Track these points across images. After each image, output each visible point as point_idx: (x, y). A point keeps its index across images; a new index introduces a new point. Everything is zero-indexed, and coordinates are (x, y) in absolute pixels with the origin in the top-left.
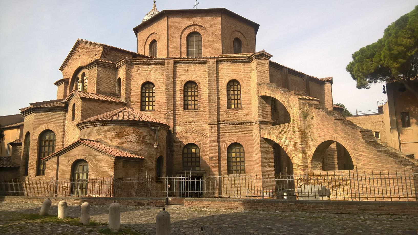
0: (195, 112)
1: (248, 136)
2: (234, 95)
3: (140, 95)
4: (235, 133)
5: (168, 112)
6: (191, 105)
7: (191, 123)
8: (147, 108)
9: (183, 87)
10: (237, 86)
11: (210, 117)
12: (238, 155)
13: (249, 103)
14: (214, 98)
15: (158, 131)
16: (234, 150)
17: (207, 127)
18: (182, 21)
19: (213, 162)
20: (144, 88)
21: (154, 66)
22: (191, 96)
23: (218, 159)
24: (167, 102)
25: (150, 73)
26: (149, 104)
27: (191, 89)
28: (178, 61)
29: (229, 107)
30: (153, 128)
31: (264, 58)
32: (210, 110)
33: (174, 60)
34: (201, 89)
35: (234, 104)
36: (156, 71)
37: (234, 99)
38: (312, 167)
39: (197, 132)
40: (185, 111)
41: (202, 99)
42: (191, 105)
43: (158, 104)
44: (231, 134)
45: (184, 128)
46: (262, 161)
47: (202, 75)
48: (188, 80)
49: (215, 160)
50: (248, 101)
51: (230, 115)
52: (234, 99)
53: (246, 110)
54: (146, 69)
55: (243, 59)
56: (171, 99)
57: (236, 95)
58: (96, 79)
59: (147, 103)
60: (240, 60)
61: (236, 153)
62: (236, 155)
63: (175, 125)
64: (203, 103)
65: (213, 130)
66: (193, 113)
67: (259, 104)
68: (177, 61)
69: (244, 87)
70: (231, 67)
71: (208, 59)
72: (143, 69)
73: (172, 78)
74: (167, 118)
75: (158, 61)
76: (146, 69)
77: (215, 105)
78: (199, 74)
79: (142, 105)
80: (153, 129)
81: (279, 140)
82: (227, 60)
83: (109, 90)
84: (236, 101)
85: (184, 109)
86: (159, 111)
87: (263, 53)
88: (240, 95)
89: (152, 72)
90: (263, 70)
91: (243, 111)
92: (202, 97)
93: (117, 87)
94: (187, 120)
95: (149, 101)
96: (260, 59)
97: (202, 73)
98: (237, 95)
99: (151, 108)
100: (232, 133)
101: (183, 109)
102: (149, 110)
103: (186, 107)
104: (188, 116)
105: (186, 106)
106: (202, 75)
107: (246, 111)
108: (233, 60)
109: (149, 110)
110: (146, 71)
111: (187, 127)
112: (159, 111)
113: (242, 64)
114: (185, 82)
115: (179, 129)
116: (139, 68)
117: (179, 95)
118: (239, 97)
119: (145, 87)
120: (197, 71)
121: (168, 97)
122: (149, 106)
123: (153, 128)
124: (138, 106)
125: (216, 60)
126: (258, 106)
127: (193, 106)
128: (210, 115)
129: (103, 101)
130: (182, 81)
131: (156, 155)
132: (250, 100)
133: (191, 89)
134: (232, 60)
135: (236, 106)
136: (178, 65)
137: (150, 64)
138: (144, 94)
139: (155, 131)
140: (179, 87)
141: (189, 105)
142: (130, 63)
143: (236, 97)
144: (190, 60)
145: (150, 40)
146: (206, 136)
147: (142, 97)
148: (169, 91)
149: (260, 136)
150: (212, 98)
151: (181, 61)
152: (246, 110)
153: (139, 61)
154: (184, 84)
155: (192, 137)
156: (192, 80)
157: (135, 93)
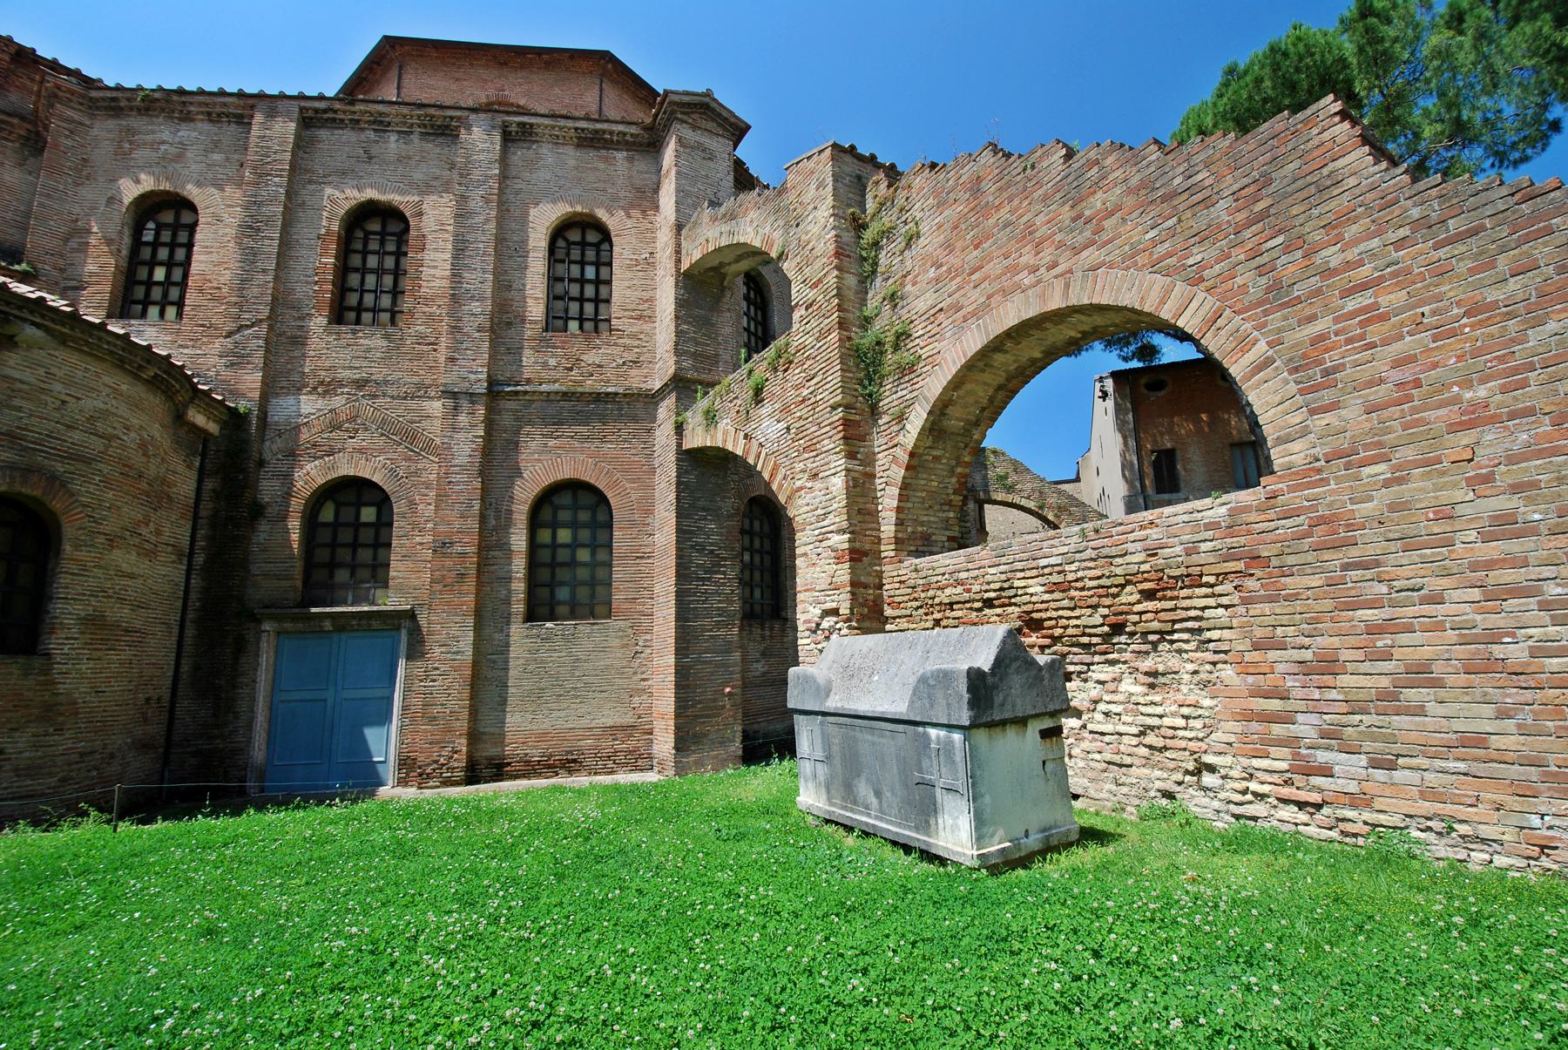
0: (387, 337)
1: (633, 451)
2: (582, 281)
4: (572, 437)
5: (240, 328)
7: (360, 384)
10: (597, 246)
11: (452, 360)
12: (585, 535)
13: (645, 313)
14: (480, 279)
16: (564, 515)
18: (454, 87)
19: (448, 563)
21: (206, 126)
22: (380, 272)
23: (474, 549)
25: (179, 157)
27: (382, 243)
28: (325, 111)
29: (555, 321)
31: (711, 125)
33: (303, 104)
36: (216, 145)
37: (581, 300)
38: (900, 535)
39: (388, 429)
40: (336, 327)
41: (424, 284)
43: (201, 291)
44: (552, 443)
45: (320, 403)
46: (678, 557)
47: (434, 183)
49: (463, 555)
50: (640, 307)
52: (581, 300)
53: (627, 341)
54: (166, 136)
55: (625, 134)
56: (264, 271)
57: (589, 281)
59: (157, 293)
60: (611, 133)
61: (574, 525)
62: (575, 537)
64: (428, 301)
65: (463, 419)
66: (373, 340)
68: (316, 111)
69: (622, 251)
70: (572, 163)
71: (466, 113)
72: (149, 138)
73: (281, 176)
74: (235, 355)
75: (225, 104)
77: (478, 310)
78: (420, 176)
81: (746, 436)
82: (553, 127)
84: (589, 308)
86: (202, 326)
87: (707, 100)
88: (609, 282)
90: (707, 176)
91: (616, 344)
96: (694, 128)
97: (438, 172)
98: (598, 282)
100: (558, 437)
103: (340, 314)
104: (346, 354)
106: (434, 183)
107: (627, 348)
108: (583, 130)
110: (163, 147)
111: (338, 401)
112: (202, 326)
113: (620, 155)
116: (130, 131)
118: (603, 290)
119: (155, 221)
120: (413, 163)
121: (250, 257)
124: (99, 297)
125: (504, 122)
132: (651, 300)
133: (382, 243)
134: (576, 129)
136: (323, 134)
141: (367, 310)
142: (81, 104)
143: (589, 291)
144: (381, 114)
146: (429, 447)
149: (679, 445)
151: (335, 112)
152: (627, 341)
153: (128, 100)
155: (361, 451)
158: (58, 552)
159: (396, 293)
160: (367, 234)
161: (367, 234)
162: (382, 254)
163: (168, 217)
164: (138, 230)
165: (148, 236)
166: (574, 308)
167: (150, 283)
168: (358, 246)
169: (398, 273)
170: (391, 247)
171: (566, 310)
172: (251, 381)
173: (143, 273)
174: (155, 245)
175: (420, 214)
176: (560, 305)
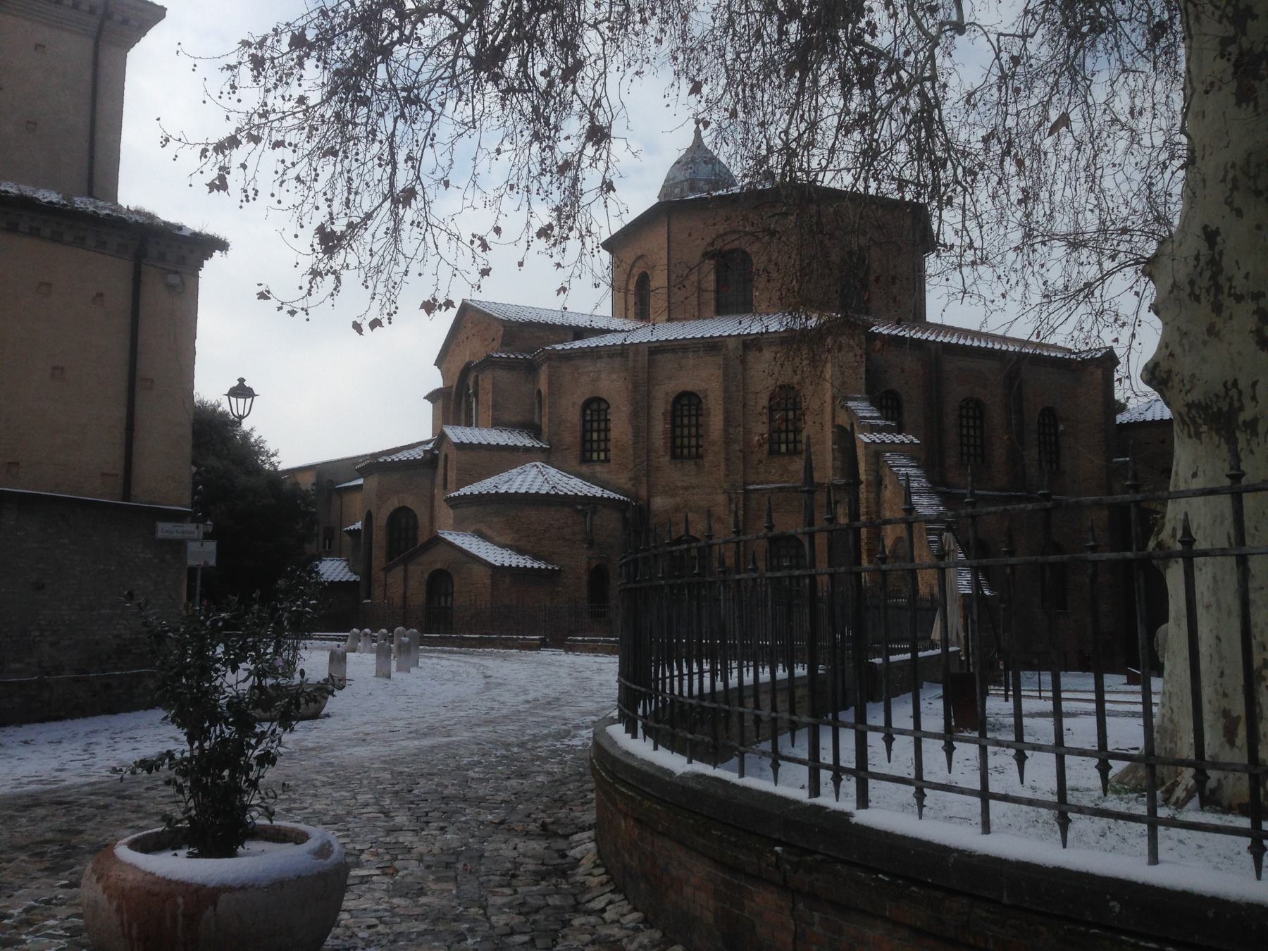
0: (696, 464)
3: (579, 428)
6: (689, 447)
7: (686, 488)
8: (595, 456)
9: (669, 408)
11: (727, 476)
15: (594, 513)
17: (721, 498)
20: (589, 412)
26: (599, 446)
27: (689, 410)
30: (579, 507)
32: (727, 460)
35: (787, 443)
37: (787, 431)
42: (689, 447)
43: (616, 447)
48: (681, 388)
51: (773, 471)
54: (591, 368)
58: (490, 395)
59: (595, 446)
63: (650, 495)
67: (834, 443)
76: (591, 368)
79: (584, 451)
80: (581, 510)
85: (674, 456)
89: (603, 376)
93: (537, 411)
95: (599, 440)
99: (602, 456)
101: (668, 458)
103: (677, 453)
111: (678, 499)
115: (659, 502)
117: (660, 427)
122: (599, 451)
123: (579, 507)
126: (833, 450)
127: (694, 450)
129: (498, 447)
130: (667, 394)
133: (689, 410)
136: (659, 357)
137: (600, 357)
140: (660, 408)
145: (636, 272)
147: (584, 432)
150: (731, 430)
154: (671, 400)
156: (689, 388)
157: (569, 425)
159: (698, 436)
160: (682, 406)
162: (690, 416)
163: (595, 406)
164: (584, 414)
165: (588, 418)
166: (783, 436)
167: (592, 441)
168: (678, 413)
169: (698, 426)
170: (693, 412)
171: (779, 438)
173: (588, 437)
174: (592, 421)
175: (706, 396)
176: (776, 436)
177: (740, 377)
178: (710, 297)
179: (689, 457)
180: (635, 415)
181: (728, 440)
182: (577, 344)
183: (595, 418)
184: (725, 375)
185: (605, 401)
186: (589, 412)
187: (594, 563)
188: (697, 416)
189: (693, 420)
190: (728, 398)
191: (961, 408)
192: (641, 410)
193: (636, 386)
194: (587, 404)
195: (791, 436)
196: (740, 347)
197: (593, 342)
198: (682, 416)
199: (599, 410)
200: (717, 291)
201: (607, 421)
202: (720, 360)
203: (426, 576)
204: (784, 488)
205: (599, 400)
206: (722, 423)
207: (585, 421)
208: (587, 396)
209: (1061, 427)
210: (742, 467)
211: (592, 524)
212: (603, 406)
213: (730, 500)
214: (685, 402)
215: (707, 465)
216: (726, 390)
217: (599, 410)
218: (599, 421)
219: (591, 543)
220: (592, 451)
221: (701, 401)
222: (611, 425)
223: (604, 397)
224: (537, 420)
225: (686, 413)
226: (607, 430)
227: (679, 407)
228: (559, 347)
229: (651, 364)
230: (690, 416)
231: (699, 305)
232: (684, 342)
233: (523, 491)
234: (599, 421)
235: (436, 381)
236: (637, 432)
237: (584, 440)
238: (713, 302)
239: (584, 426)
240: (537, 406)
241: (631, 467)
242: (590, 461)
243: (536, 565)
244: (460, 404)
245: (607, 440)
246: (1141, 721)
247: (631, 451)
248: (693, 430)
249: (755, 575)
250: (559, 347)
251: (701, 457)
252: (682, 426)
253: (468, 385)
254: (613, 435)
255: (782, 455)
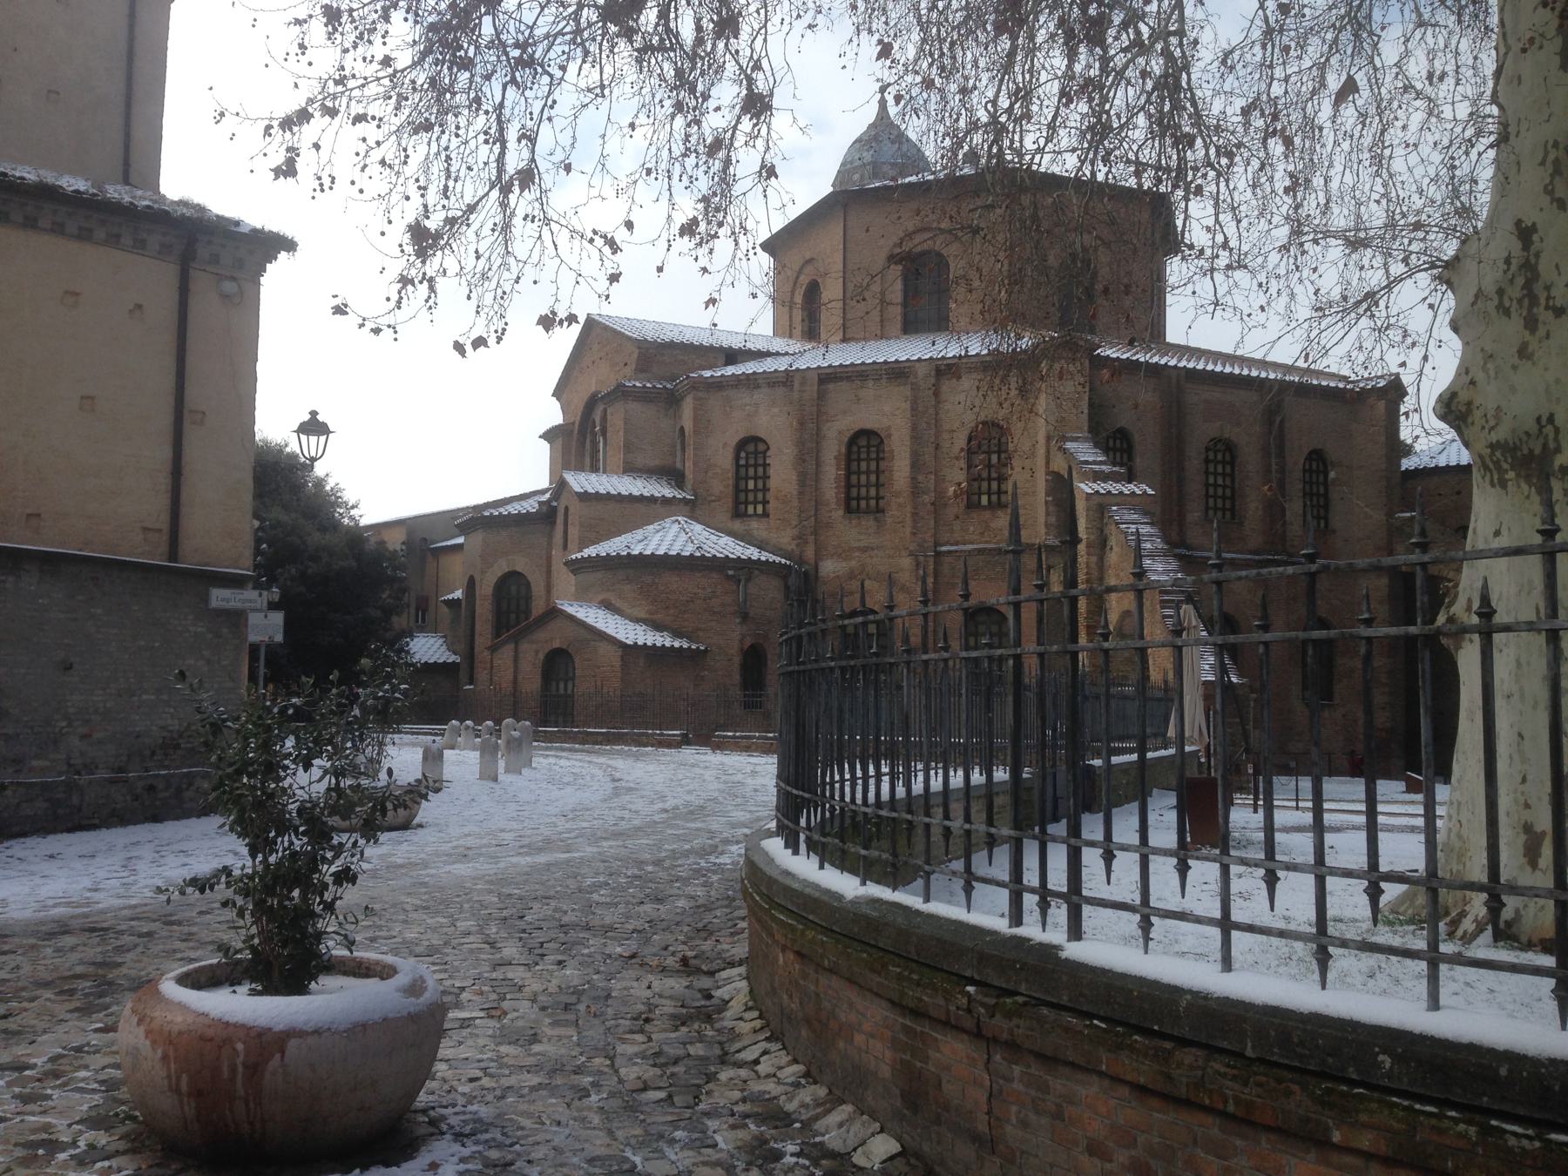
0: (876, 519)
6: (867, 498)
7: (864, 550)
8: (751, 509)
9: (843, 450)
15: (748, 580)
16: (982, 628)
17: (906, 562)
20: (743, 454)
24: (800, 493)
26: (755, 497)
27: (868, 453)
32: (915, 514)
34: (892, 451)
37: (990, 479)
42: (867, 498)
43: (777, 498)
45: (844, 564)
48: (857, 427)
58: (621, 433)
66: (869, 522)
67: (1047, 495)
79: (737, 502)
83: (657, 462)
85: (849, 510)
92: (896, 475)
93: (679, 453)
94: (857, 545)
95: (756, 490)
99: (760, 509)
101: (841, 512)
102: (755, 514)
103: (851, 505)
105: (854, 503)
109: (755, 514)
111: (853, 563)
114: (848, 435)
115: (829, 567)
117: (831, 473)
122: (755, 503)
126: (1046, 502)
127: (873, 502)
128: (914, 527)
129: (631, 499)
131: (742, 641)
133: (868, 453)
135: (994, 498)
136: (831, 386)
137: (758, 387)
138: (743, 471)
139: (739, 581)
140: (832, 450)
145: (804, 280)
147: (738, 478)
148: (804, 461)
150: (920, 478)
156: (868, 426)
157: (719, 471)
158: (766, 665)
159: (878, 485)
161: (859, 448)
162: (868, 460)
163: (751, 448)
164: (737, 458)
165: (742, 462)
166: (985, 485)
167: (747, 491)
168: (854, 456)
169: (878, 472)
170: (873, 456)
172: (810, 553)
174: (747, 466)
175: (890, 436)
176: (976, 484)
177: (932, 411)
178: (896, 312)
179: (868, 511)
180: (801, 459)
181: (916, 490)
182: (730, 370)
183: (752, 461)
184: (914, 409)
185: (764, 442)
186: (743, 454)
187: (748, 642)
188: (878, 460)
189: (873, 465)
190: (916, 436)
191: (1207, 449)
192: (808, 454)
193: (802, 424)
194: (742, 444)
195: (994, 485)
196: (933, 373)
197: (750, 367)
198: (859, 460)
199: (756, 453)
200: (905, 304)
201: (765, 465)
202: (906, 391)
203: (541, 656)
204: (985, 549)
205: (756, 440)
206: (908, 469)
207: (738, 466)
208: (742, 435)
209: (1332, 475)
210: (932, 522)
211: (746, 593)
212: (761, 447)
213: (918, 565)
214: (863, 442)
215: (889, 520)
216: (914, 428)
217: (756, 453)
218: (756, 466)
219: (745, 617)
220: (746, 503)
221: (882, 441)
222: (771, 472)
223: (762, 435)
224: (679, 465)
225: (863, 456)
226: (766, 477)
227: (855, 449)
228: (707, 374)
229: (821, 396)
230: (868, 460)
231: (882, 321)
232: (863, 368)
233: (661, 552)
234: (756, 466)
235: (554, 415)
236: (802, 483)
237: (737, 490)
238: (899, 318)
239: (737, 472)
240: (679, 447)
241: (794, 523)
242: (745, 515)
243: (677, 644)
244: (583, 444)
245: (765, 490)
246: (1422, 837)
247: (796, 503)
248: (873, 478)
249: (946, 655)
250: (707, 374)
251: (883, 511)
252: (859, 473)
253: (594, 422)
254: (773, 483)
255: (985, 508)
